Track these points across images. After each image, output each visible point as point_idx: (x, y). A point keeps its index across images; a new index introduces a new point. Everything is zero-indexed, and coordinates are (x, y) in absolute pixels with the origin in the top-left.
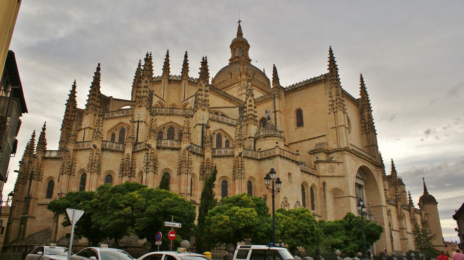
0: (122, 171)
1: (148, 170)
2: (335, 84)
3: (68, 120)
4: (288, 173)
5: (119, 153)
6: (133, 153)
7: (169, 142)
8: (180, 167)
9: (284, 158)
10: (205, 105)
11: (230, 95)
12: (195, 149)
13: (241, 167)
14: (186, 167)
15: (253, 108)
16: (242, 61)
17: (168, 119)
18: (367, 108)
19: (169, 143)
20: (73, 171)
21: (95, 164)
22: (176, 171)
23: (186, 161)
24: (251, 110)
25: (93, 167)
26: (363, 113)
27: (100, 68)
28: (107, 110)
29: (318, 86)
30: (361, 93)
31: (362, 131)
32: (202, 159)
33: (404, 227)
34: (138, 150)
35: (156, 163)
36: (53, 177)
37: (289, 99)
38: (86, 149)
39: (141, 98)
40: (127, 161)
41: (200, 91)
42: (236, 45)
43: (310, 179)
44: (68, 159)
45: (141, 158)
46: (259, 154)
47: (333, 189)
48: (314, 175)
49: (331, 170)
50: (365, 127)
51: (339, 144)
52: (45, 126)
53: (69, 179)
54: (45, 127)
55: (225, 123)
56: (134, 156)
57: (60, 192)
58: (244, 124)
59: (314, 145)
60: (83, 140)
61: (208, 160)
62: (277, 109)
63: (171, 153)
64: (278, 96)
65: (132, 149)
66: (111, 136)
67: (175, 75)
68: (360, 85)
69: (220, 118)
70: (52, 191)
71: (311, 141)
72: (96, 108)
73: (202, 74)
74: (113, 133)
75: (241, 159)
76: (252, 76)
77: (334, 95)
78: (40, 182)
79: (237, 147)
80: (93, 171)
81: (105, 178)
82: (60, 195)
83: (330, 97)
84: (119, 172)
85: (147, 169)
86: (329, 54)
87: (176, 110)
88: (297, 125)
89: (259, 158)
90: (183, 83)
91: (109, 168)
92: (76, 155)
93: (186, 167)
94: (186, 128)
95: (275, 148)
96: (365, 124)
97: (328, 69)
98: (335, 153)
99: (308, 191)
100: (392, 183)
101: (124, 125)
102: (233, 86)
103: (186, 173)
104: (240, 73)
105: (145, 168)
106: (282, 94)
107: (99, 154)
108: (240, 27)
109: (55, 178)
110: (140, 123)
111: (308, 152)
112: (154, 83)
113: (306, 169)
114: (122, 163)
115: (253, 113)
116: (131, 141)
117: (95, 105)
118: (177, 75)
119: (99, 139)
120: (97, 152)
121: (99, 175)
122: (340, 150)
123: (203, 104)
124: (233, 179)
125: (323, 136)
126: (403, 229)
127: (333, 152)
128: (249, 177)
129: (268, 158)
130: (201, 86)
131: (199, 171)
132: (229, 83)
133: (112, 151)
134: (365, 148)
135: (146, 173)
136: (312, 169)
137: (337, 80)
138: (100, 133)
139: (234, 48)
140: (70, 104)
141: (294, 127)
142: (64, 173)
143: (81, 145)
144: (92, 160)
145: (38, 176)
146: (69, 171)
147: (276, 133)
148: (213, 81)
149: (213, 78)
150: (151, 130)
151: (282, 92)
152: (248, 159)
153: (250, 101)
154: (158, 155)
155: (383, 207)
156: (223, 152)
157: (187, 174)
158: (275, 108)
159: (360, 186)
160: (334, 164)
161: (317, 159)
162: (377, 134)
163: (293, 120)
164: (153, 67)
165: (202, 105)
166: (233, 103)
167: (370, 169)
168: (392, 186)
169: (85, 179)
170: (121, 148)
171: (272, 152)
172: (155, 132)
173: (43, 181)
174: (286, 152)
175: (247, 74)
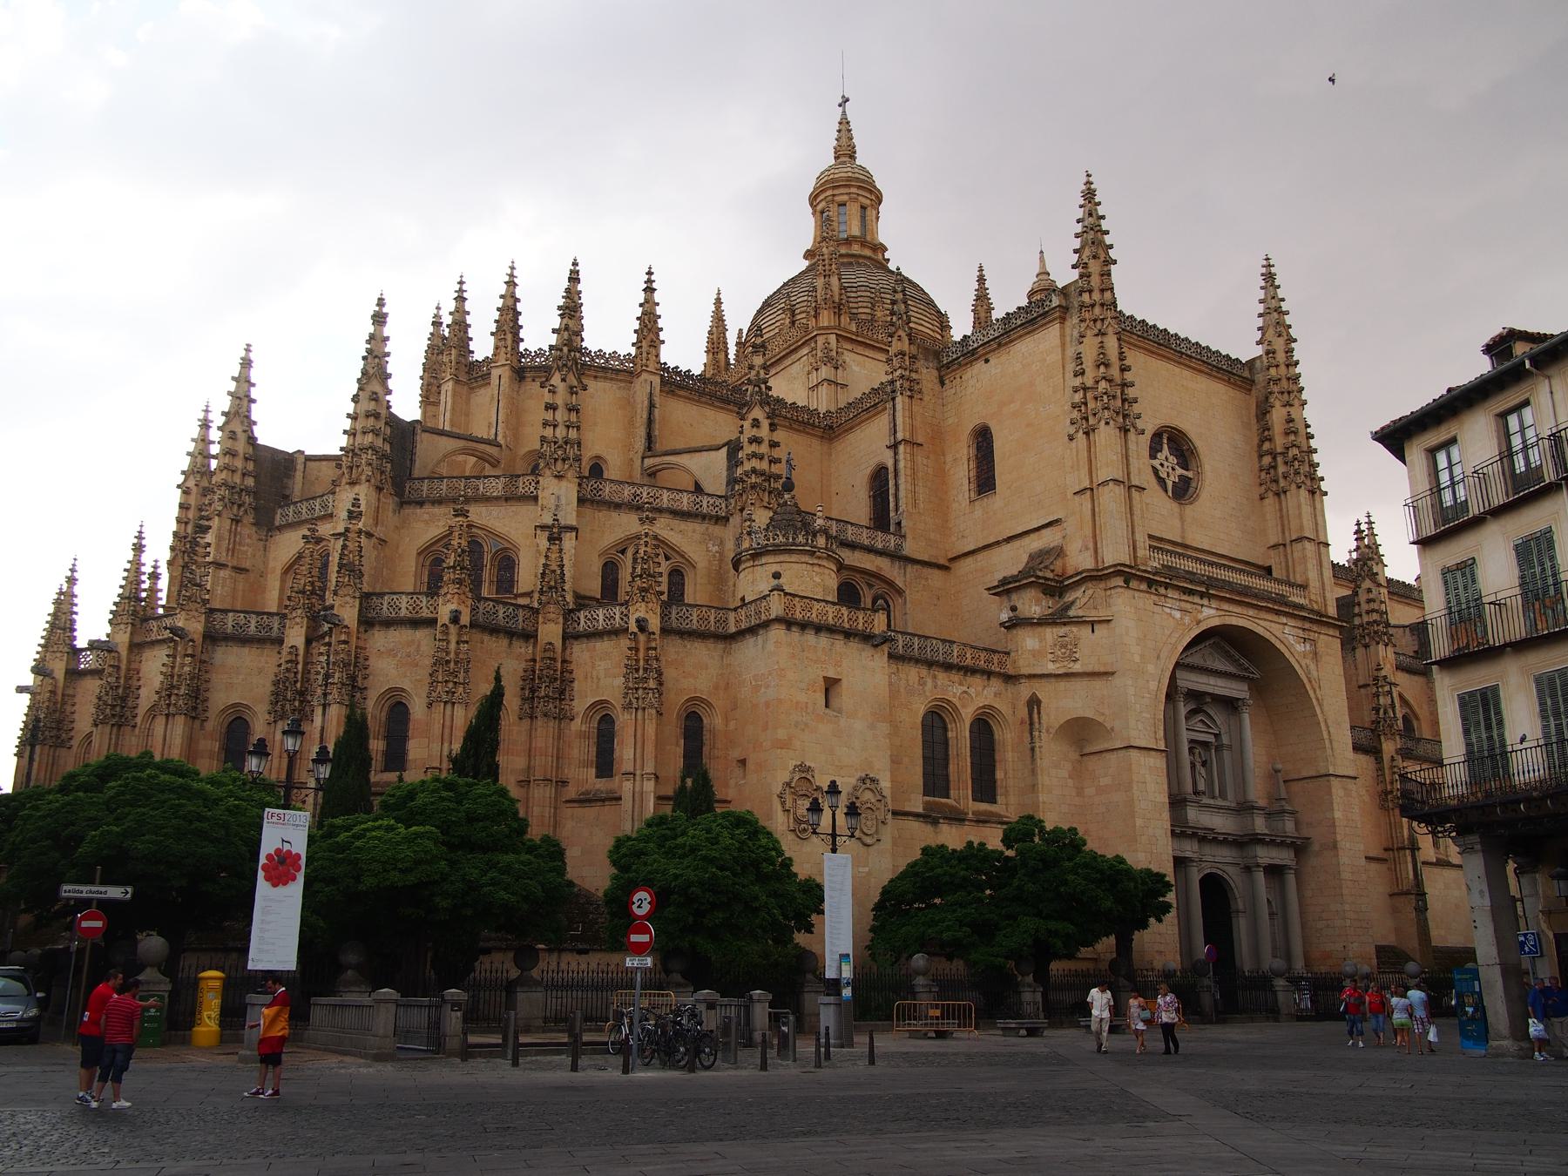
2: (1095, 321)
3: (185, 537)
5: (268, 646)
6: (308, 642)
10: (564, 460)
12: (501, 615)
13: (645, 670)
14: (446, 682)
15: (764, 449)
16: (823, 260)
18: (1282, 393)
19: (404, 605)
20: (128, 714)
21: (179, 689)
22: (424, 695)
23: (448, 662)
24: (754, 455)
25: (173, 698)
29: (1038, 336)
30: (1263, 335)
31: (1261, 485)
37: (953, 391)
40: (288, 670)
43: (972, 691)
44: (110, 675)
46: (732, 616)
47: (1068, 721)
48: (989, 674)
49: (1063, 650)
50: (1275, 467)
51: (1100, 551)
52: (73, 570)
53: (117, 738)
58: (734, 508)
59: (1025, 558)
61: (549, 650)
62: (900, 436)
63: (410, 638)
64: (906, 384)
65: (305, 628)
67: (540, 349)
68: (1261, 302)
71: (1016, 544)
73: (561, 350)
75: (649, 640)
76: (868, 311)
77: (1090, 364)
78: (62, 752)
80: (172, 710)
83: (1075, 376)
84: (270, 707)
85: (325, 695)
86: (1081, 206)
88: (979, 486)
89: (733, 629)
94: (455, 551)
96: (1274, 458)
97: (1074, 267)
99: (960, 737)
103: (446, 703)
104: (814, 305)
106: (927, 375)
107: (192, 656)
108: (844, 123)
111: (989, 589)
112: (475, 385)
113: (955, 654)
116: (304, 604)
117: (233, 488)
119: (193, 606)
120: (186, 650)
121: (197, 723)
122: (1100, 574)
125: (1050, 524)
127: (1078, 584)
128: (688, 701)
129: (752, 630)
130: (554, 392)
133: (243, 640)
134: (1272, 552)
135: (320, 708)
137: (1102, 305)
139: (819, 208)
140: (191, 483)
143: (155, 629)
146: (113, 716)
147: (794, 539)
151: (925, 371)
152: (685, 636)
153: (756, 424)
155: (1335, 782)
156: (601, 618)
157: (449, 706)
160: (1075, 629)
161: (1011, 615)
162: (1326, 494)
163: (961, 471)
164: (469, 326)
165: (556, 460)
167: (1267, 635)
173: (75, 748)
174: (817, 606)
175: (838, 309)
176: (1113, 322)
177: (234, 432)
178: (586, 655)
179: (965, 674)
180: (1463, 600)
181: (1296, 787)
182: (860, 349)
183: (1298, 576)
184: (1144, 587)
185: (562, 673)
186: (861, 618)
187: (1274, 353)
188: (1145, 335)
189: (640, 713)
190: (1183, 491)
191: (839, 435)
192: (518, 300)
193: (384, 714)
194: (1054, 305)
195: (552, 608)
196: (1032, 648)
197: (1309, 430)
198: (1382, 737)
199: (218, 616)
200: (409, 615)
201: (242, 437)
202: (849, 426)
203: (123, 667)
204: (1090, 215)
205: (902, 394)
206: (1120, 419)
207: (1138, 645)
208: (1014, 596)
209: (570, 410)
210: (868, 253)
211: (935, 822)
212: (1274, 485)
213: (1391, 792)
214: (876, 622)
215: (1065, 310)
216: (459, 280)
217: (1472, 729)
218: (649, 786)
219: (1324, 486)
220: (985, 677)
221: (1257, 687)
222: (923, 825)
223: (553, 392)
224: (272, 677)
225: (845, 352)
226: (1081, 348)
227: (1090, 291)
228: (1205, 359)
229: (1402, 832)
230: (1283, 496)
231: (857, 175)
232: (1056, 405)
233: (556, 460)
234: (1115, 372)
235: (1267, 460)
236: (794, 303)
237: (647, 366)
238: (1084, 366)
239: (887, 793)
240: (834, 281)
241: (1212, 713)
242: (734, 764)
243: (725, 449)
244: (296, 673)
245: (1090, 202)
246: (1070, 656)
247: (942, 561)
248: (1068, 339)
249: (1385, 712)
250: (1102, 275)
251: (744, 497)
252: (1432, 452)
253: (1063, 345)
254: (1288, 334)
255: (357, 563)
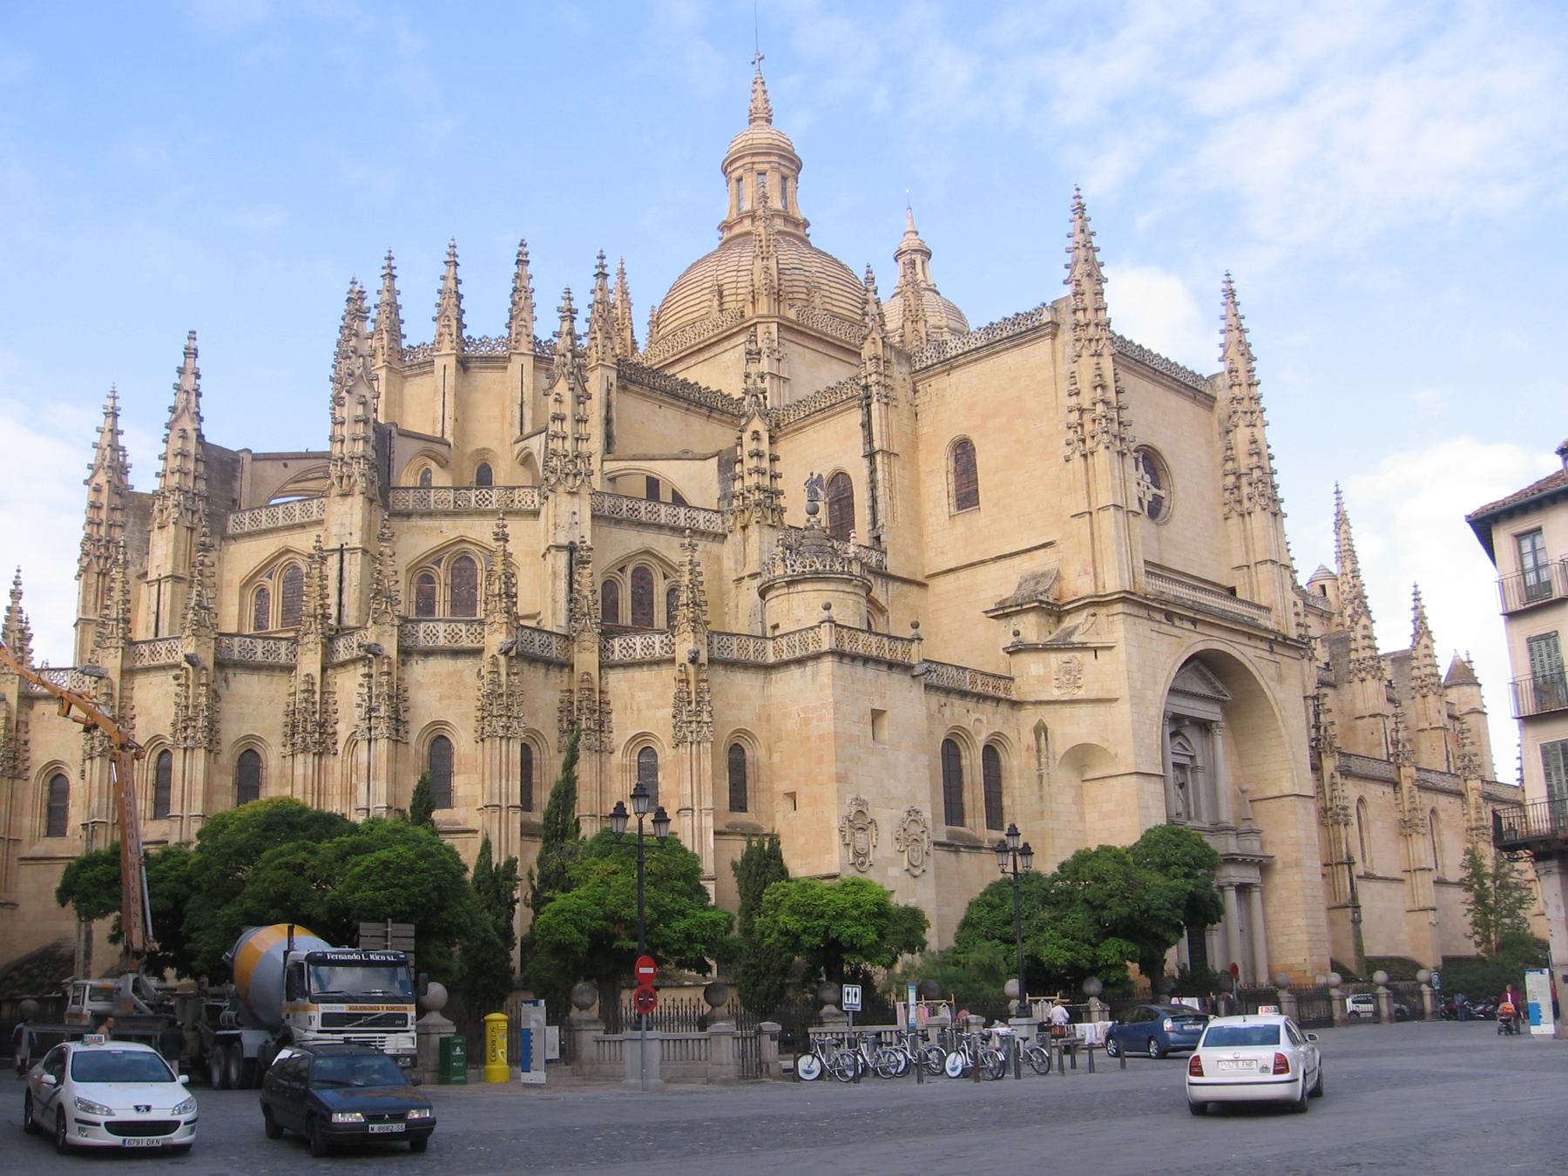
0: (294, 734)
1: (373, 732)
4: (873, 710)
5: (277, 674)
6: (324, 670)
7: (443, 629)
8: (485, 714)
9: (854, 658)
11: (707, 388)
12: (537, 643)
13: (698, 703)
14: (501, 716)
15: (765, 464)
16: (760, 241)
17: (450, 530)
19: (441, 634)
26: (1231, 434)
27: (196, 350)
28: (234, 501)
30: (1225, 352)
31: (1225, 504)
32: (566, 679)
33: (1424, 866)
34: (341, 659)
35: (400, 706)
36: (61, 762)
38: (163, 668)
39: (347, 463)
40: (306, 700)
41: (558, 423)
42: (743, 165)
43: (984, 719)
45: (349, 687)
46: (770, 644)
48: (998, 700)
49: (1068, 677)
50: (1238, 488)
54: (20, 587)
55: (660, 527)
56: (330, 680)
57: (89, 819)
60: (156, 635)
64: (883, 392)
66: (254, 598)
69: (643, 509)
70: (65, 809)
72: (194, 502)
73: (565, 356)
74: (259, 589)
78: (18, 783)
79: (681, 630)
81: (235, 764)
82: (90, 829)
83: (1070, 395)
85: (370, 729)
87: (478, 493)
88: (958, 500)
89: (771, 659)
90: (514, 367)
91: (246, 730)
92: (132, 689)
93: (501, 716)
95: (819, 627)
96: (1239, 477)
98: (1085, 613)
100: (1413, 684)
101: (297, 557)
102: (726, 345)
103: (501, 738)
104: (751, 288)
105: (364, 725)
109: (67, 766)
110: (347, 556)
111: (986, 612)
114: (291, 708)
115: (766, 482)
116: (317, 630)
117: (187, 492)
118: (493, 335)
120: (199, 678)
121: (212, 755)
123: (567, 471)
124: (674, 744)
125: (1044, 546)
126: (1418, 873)
127: (1078, 609)
129: (800, 662)
130: (561, 402)
131: (556, 721)
132: (711, 334)
133: (256, 668)
134: (1237, 573)
136: (991, 680)
137: (1097, 325)
138: (207, 609)
139: (736, 175)
140: (102, 479)
141: (946, 509)
142: (95, 754)
143: (147, 653)
144: (187, 707)
145: (11, 763)
147: (831, 566)
148: (655, 322)
149: (653, 307)
150: (376, 594)
153: (756, 436)
154: (406, 677)
156: (638, 647)
158: (871, 441)
159: (1205, 725)
160: (1078, 655)
161: (1015, 639)
162: (1286, 516)
163: (938, 483)
164: (400, 307)
165: (567, 474)
166: (720, 420)
168: (1413, 692)
169: (168, 769)
170: (283, 655)
171: (810, 641)
172: (390, 597)
173: (33, 780)
174: (861, 636)
175: (778, 296)
176: (1108, 343)
177: (184, 431)
178: (624, 685)
179: (978, 702)
180: (1547, 667)
181: (1258, 805)
182: (799, 339)
183: (1262, 598)
184: (1188, 625)
185: (600, 703)
186: (899, 648)
187: (1236, 371)
188: (1124, 351)
189: (694, 746)
190: (1155, 509)
191: (786, 434)
192: (458, 282)
193: (426, 748)
194: (1045, 321)
195: (586, 636)
196: (1036, 676)
197: (1270, 451)
198: (1323, 755)
199: (226, 641)
200: (448, 644)
201: (193, 436)
202: (799, 425)
203: (117, 694)
204: (1082, 231)
205: (878, 401)
206: (1118, 443)
207: (1139, 671)
208: (1014, 620)
209: (578, 421)
210: (790, 229)
211: (957, 851)
212: (1238, 505)
213: (1331, 809)
214: (912, 651)
215: (1055, 325)
216: (387, 255)
217: (1553, 773)
218: (709, 822)
219: (1284, 508)
220: (995, 704)
221: (1229, 710)
222: (947, 854)
223: (559, 401)
224: (283, 707)
225: (786, 342)
226: (1074, 367)
227: (1085, 310)
228: (1174, 375)
229: (1340, 847)
230: (1247, 516)
231: (778, 143)
232: (1052, 425)
233: (567, 474)
234: (1111, 395)
235: (1231, 480)
236: (722, 282)
237: (603, 360)
238: (1078, 386)
239: (929, 825)
240: (772, 263)
241: (1188, 735)
242: (781, 798)
243: (714, 462)
244: (314, 703)
245: (1081, 217)
246: (1074, 683)
247: (919, 578)
248: (1059, 356)
249: (1325, 731)
250: (1096, 294)
251: (747, 514)
252: (1519, 537)
253: (1054, 361)
254: (1249, 353)
255: (393, 588)
